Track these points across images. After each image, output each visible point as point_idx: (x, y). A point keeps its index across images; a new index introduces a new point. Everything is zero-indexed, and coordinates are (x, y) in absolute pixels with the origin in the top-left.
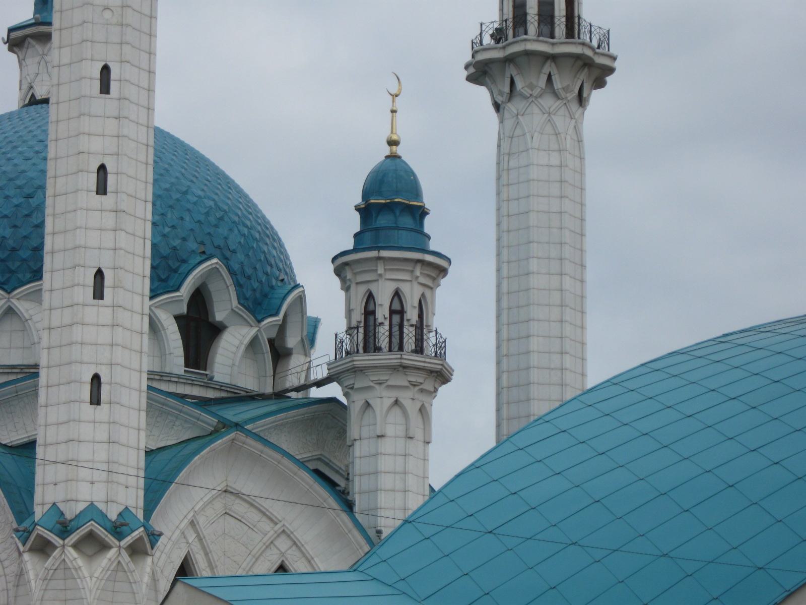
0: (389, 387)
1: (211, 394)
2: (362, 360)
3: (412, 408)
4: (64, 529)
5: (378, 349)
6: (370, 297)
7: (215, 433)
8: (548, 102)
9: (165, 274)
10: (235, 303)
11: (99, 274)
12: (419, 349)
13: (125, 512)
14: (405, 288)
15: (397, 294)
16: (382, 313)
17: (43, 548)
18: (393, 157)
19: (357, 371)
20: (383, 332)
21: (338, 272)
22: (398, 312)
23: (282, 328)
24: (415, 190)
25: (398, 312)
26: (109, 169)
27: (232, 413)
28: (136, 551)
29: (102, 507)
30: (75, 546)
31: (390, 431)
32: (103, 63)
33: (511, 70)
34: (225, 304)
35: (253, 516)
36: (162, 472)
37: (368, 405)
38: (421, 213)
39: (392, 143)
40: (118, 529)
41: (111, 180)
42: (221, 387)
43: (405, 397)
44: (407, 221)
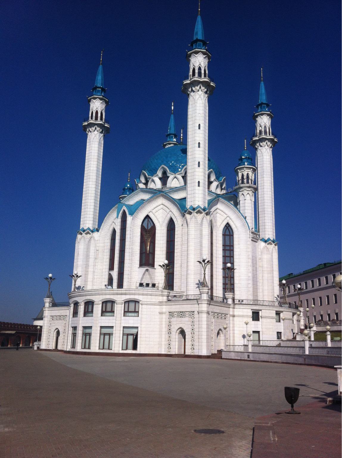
0: (247, 191)
4: (194, 209)
5: (245, 184)
6: (243, 175)
10: (215, 178)
13: (205, 207)
14: (249, 172)
15: (248, 174)
16: (245, 177)
17: (190, 213)
20: (245, 181)
26: (200, 143)
29: (200, 206)
30: (196, 213)
31: (247, 199)
32: (199, 124)
35: (222, 213)
37: (243, 194)
40: (204, 210)
41: (201, 145)
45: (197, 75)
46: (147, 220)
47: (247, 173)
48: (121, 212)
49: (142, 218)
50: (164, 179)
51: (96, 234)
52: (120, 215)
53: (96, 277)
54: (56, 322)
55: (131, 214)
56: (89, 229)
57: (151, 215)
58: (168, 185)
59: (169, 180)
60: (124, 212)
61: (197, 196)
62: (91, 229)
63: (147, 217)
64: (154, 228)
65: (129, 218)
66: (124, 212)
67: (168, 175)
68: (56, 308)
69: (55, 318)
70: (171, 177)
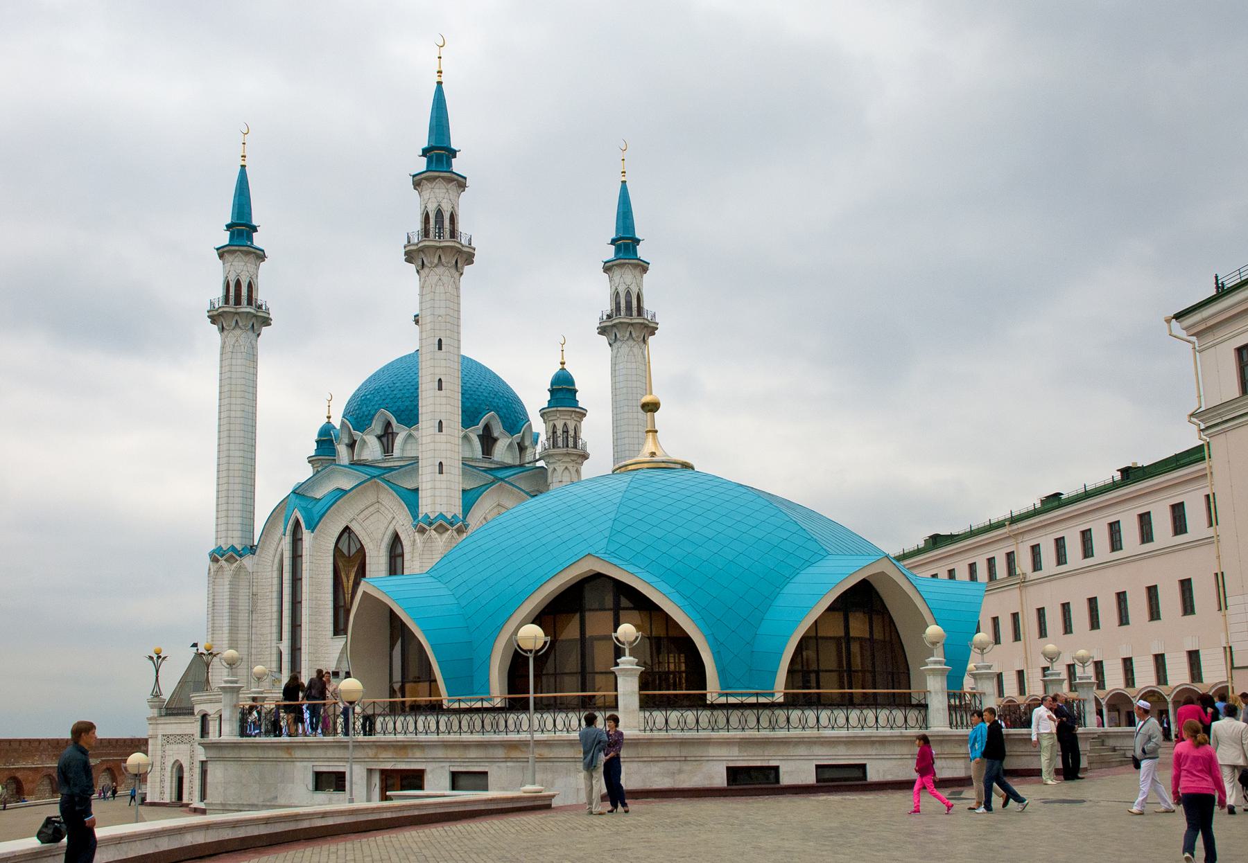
1: (493, 466)
2: (552, 451)
3: (573, 470)
7: (493, 483)
8: (631, 342)
9: (469, 417)
12: (575, 446)
13: (454, 516)
14: (569, 422)
16: (559, 432)
17: (422, 531)
18: (563, 369)
19: (549, 456)
20: (560, 440)
21: (542, 416)
22: (566, 432)
23: (523, 438)
24: (573, 383)
25: (566, 432)
27: (501, 474)
28: (460, 531)
33: (615, 330)
34: (497, 430)
36: (469, 498)
38: (576, 391)
39: (563, 363)
42: (497, 463)
43: (570, 466)
44: (568, 395)
46: (346, 535)
47: (562, 422)
48: (291, 522)
49: (337, 535)
50: (387, 437)
51: (248, 561)
52: (289, 527)
53: (253, 651)
54: (175, 747)
55: (312, 527)
56: (233, 548)
57: (355, 527)
58: (397, 452)
59: (399, 441)
60: (297, 523)
61: (439, 493)
62: (239, 547)
63: (347, 528)
64: (362, 551)
65: (307, 536)
66: (297, 523)
68: (172, 719)
69: (171, 739)
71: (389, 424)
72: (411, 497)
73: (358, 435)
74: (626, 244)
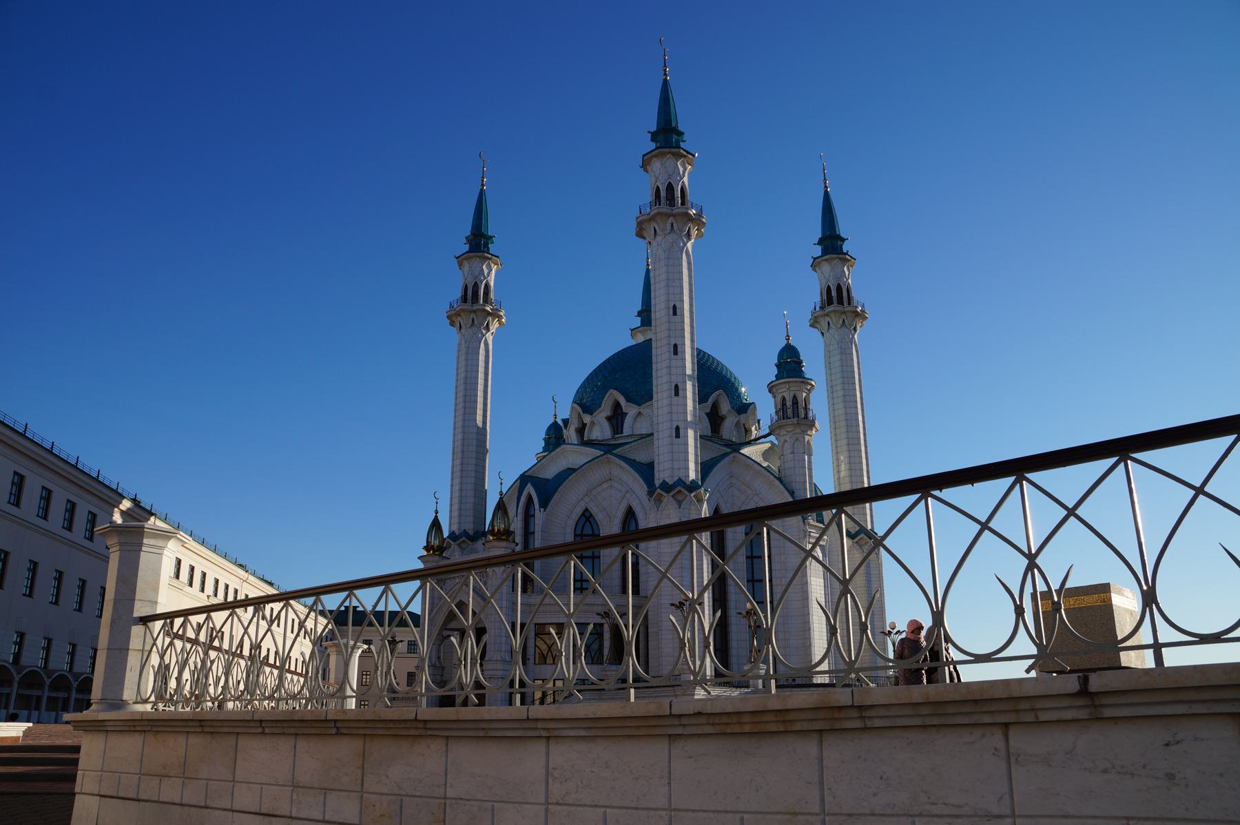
7: (726, 455)
11: (676, 386)
15: (795, 397)
16: (789, 403)
20: (790, 412)
34: (725, 407)
45: (663, 200)
47: (792, 394)
48: (523, 499)
50: (616, 418)
56: (465, 533)
59: (628, 422)
60: (530, 498)
62: (471, 533)
66: (530, 498)
67: (624, 410)
70: (631, 410)
71: (617, 405)
72: (646, 471)
73: (587, 419)
74: (832, 243)
